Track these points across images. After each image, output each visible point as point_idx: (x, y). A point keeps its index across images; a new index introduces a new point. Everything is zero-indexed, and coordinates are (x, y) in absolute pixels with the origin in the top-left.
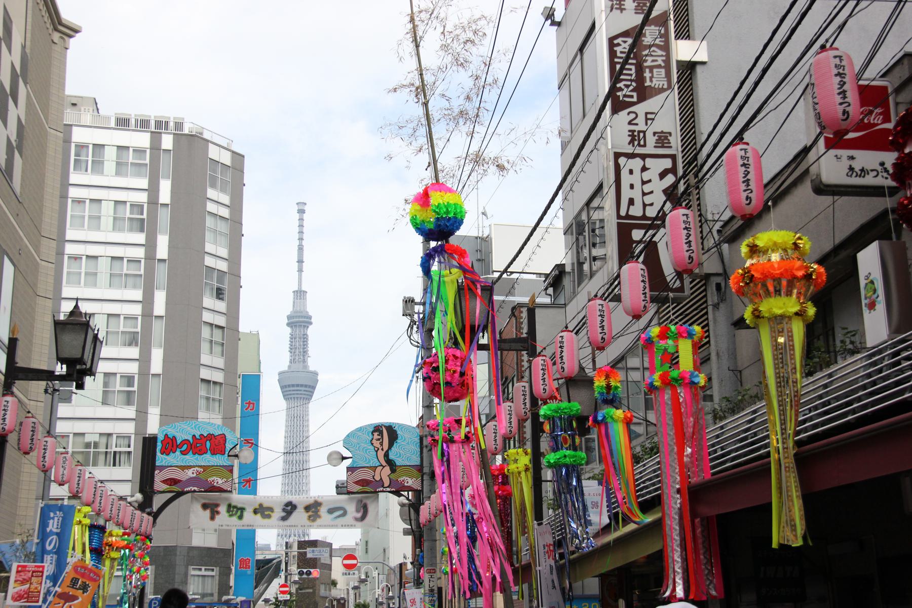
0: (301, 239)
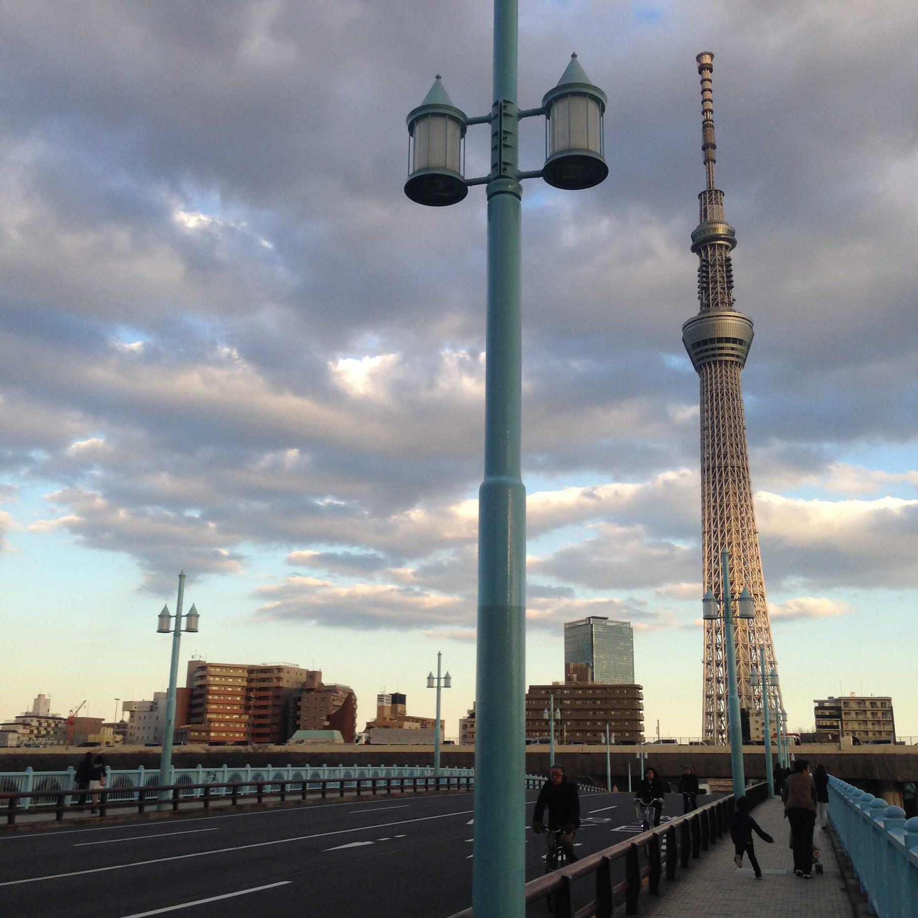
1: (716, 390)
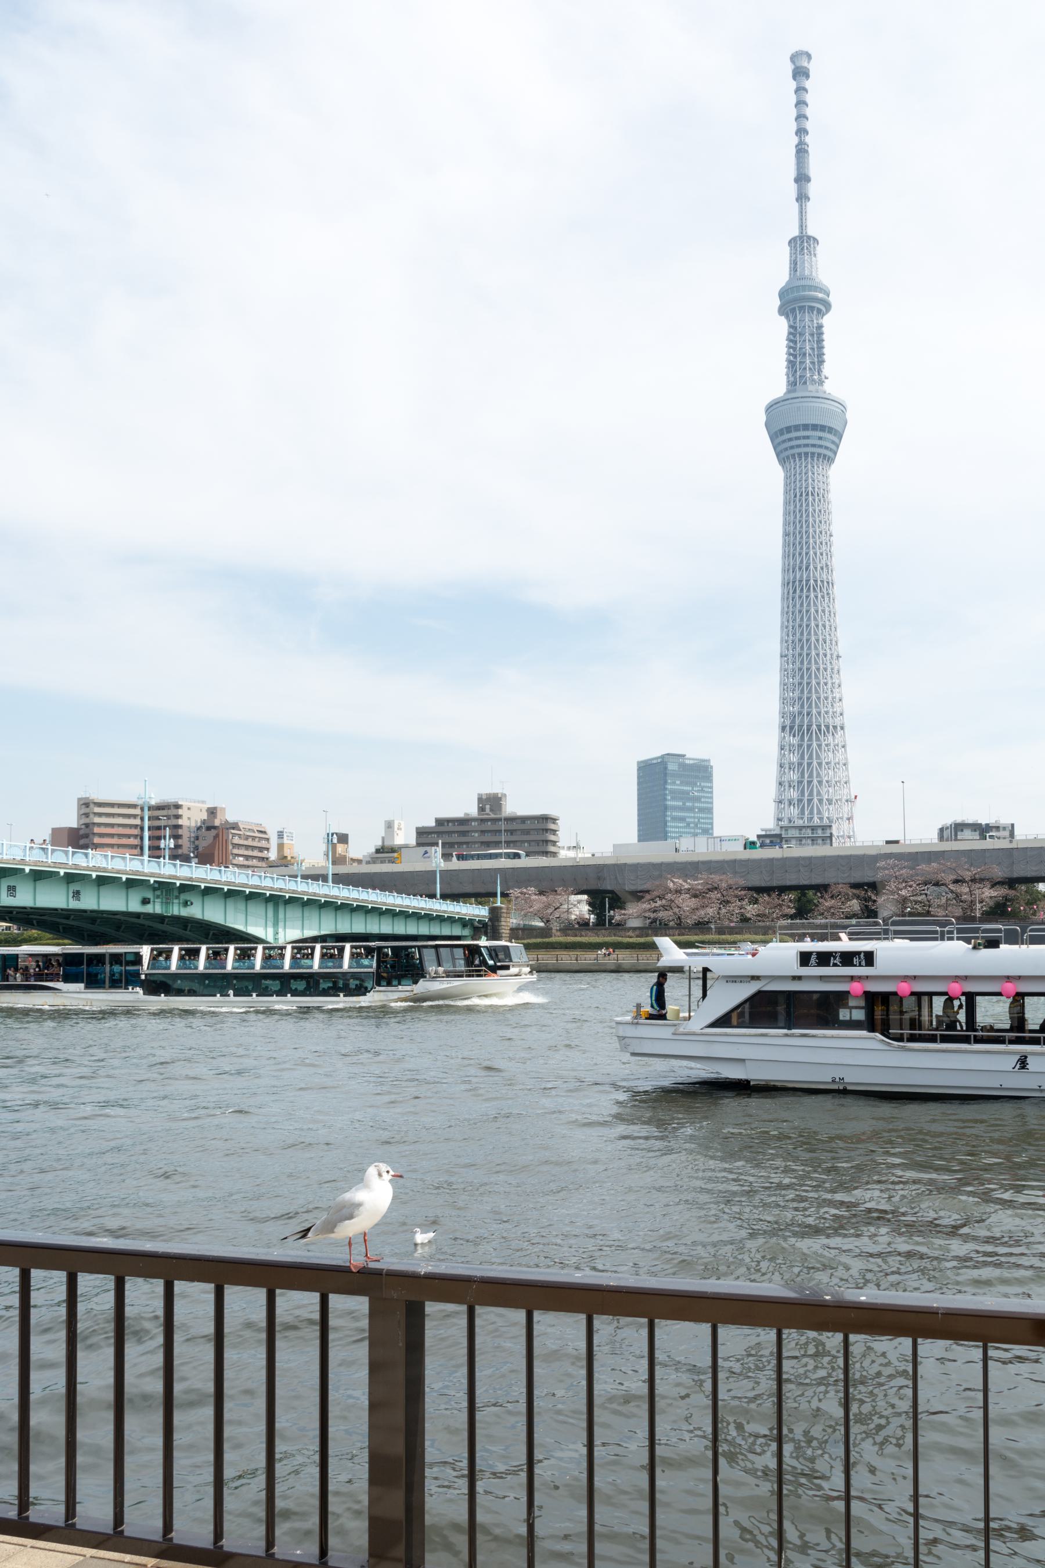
0: (801, 132)
1: (800, 488)
